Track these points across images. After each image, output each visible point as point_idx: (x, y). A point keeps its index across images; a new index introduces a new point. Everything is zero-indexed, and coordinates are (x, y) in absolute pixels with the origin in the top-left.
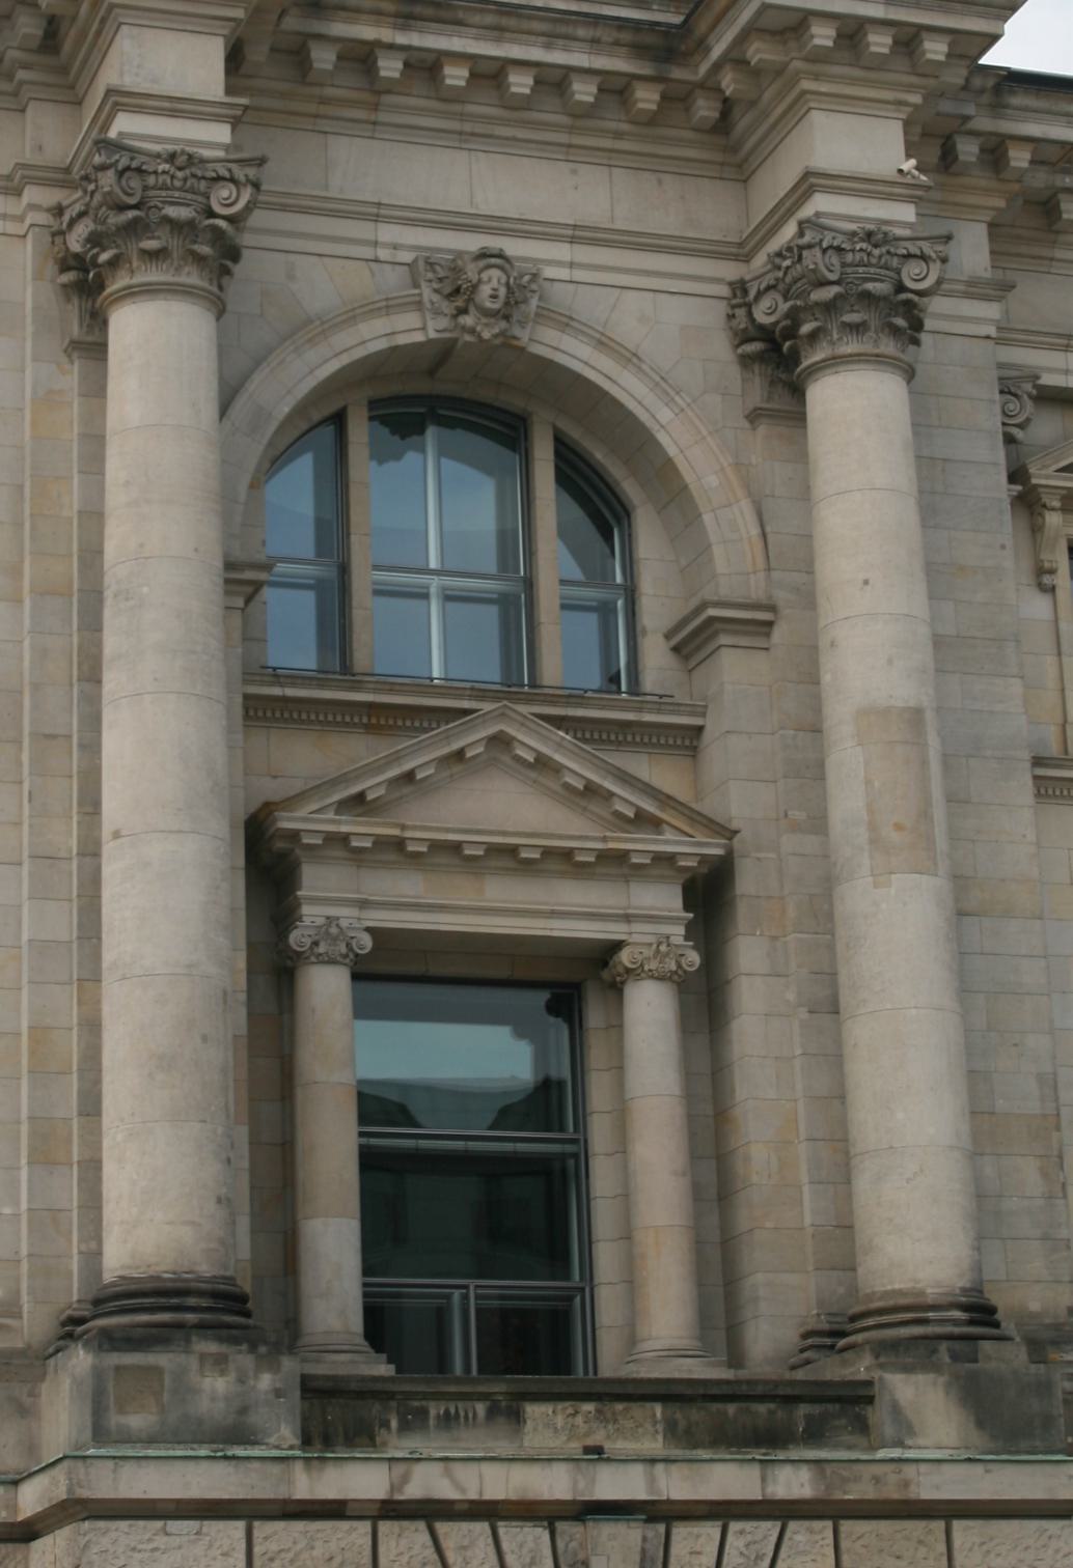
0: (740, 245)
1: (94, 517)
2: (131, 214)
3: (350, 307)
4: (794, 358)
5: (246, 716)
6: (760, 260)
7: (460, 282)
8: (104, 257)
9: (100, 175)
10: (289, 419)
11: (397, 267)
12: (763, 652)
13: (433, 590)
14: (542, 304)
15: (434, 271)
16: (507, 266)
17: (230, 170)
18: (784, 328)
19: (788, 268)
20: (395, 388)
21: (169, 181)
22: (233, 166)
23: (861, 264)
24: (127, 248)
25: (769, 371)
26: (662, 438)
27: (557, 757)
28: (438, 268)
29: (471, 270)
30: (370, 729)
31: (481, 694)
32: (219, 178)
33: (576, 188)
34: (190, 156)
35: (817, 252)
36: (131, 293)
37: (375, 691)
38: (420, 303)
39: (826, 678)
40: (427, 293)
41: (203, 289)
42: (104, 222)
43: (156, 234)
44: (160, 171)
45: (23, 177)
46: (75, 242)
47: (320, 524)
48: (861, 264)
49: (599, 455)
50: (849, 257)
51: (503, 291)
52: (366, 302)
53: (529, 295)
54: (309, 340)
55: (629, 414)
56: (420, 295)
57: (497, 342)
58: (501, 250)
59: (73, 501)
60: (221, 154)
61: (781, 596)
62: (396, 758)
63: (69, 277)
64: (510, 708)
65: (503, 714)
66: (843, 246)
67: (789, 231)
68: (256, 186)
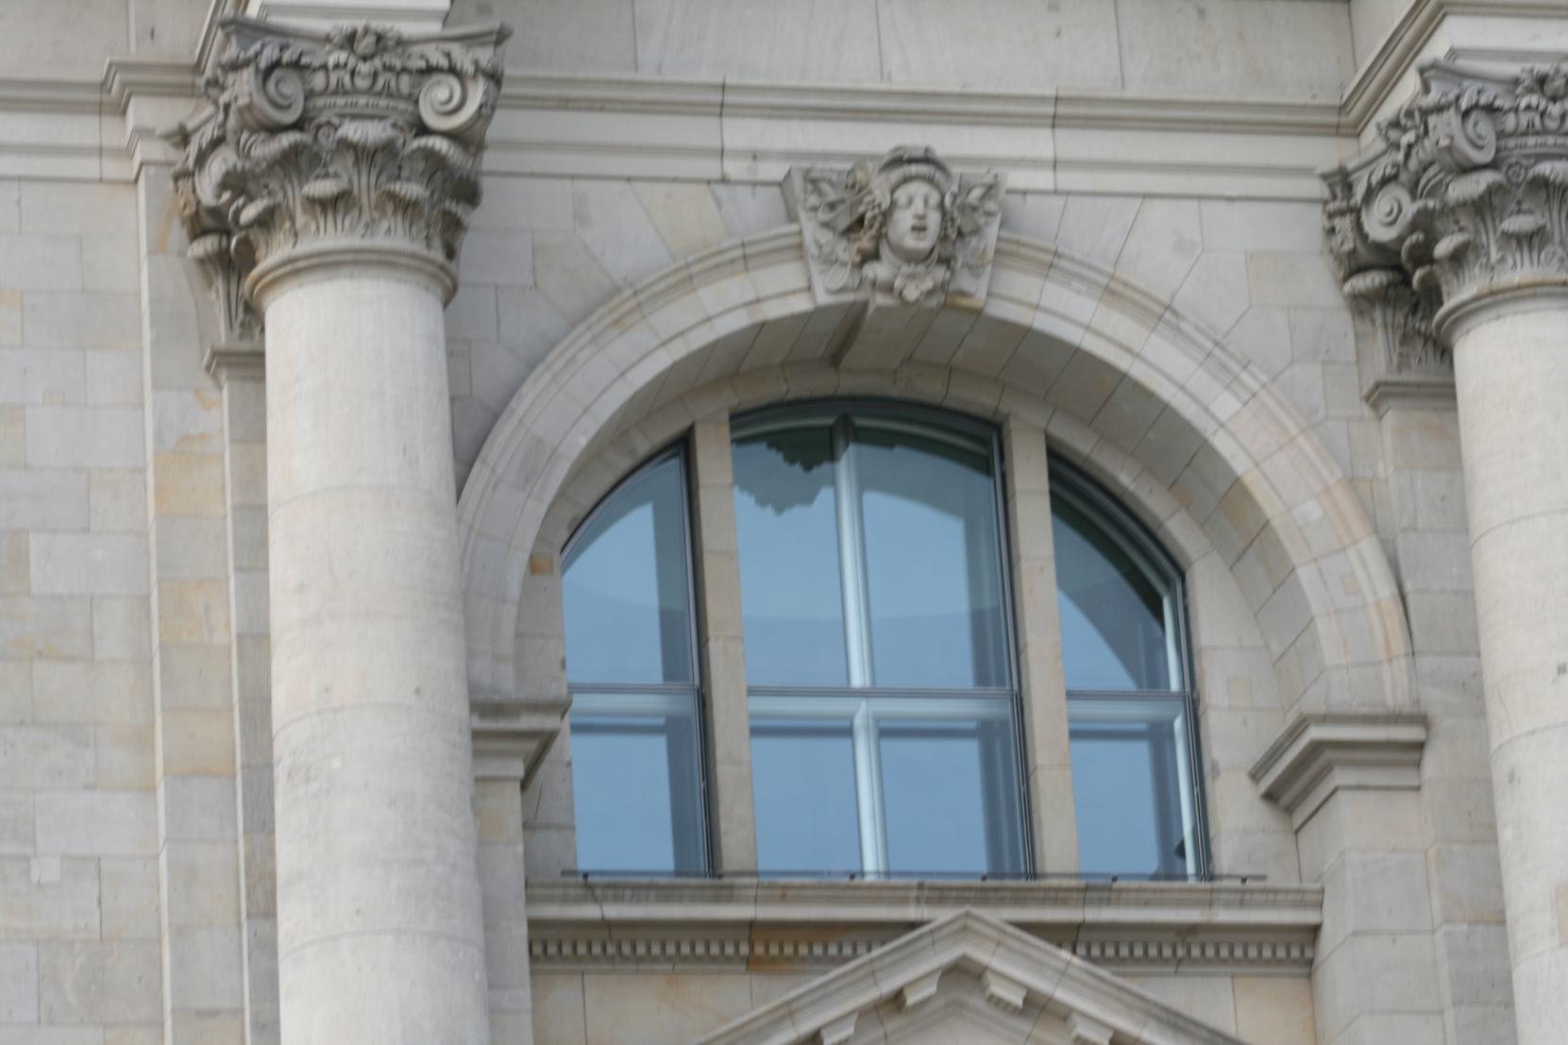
0: (1342, 109)
1: (256, 641)
2: (286, 140)
3: (681, 262)
4: (1432, 295)
5: (533, 958)
6: (1370, 133)
7: (862, 209)
8: (249, 214)
9: (231, 78)
10: (594, 454)
11: (759, 190)
12: (1410, 796)
13: (859, 722)
14: (1005, 234)
15: (820, 193)
16: (939, 176)
17: (448, 55)
18: (1414, 247)
19: (1410, 146)
20: (774, 390)
21: (347, 80)
22: (457, 50)
23: (1529, 131)
24: (285, 195)
25: (1400, 319)
26: (1222, 443)
27: (1062, 995)
28: (825, 187)
29: (879, 190)
30: (752, 963)
31: (939, 895)
32: (430, 70)
33: (1058, 34)
34: (380, 38)
35: (1452, 116)
36: (295, 270)
37: (756, 901)
38: (800, 246)
39: (1506, 835)
40: (811, 230)
41: (413, 256)
42: (248, 156)
43: (331, 170)
44: (331, 63)
45: (124, 85)
46: (207, 188)
47: (668, 621)
48: (1529, 131)
49: (1126, 477)
50: (1510, 122)
51: (934, 220)
52: (705, 253)
53: (982, 220)
54: (616, 322)
55: (1166, 408)
56: (800, 233)
57: (933, 302)
58: (927, 150)
59: (228, 621)
60: (434, 28)
61: (1435, 700)
62: (787, 1013)
63: (208, 245)
64: (978, 919)
65: (965, 928)
66: (1498, 103)
67: (1408, 88)
68: (495, 78)
